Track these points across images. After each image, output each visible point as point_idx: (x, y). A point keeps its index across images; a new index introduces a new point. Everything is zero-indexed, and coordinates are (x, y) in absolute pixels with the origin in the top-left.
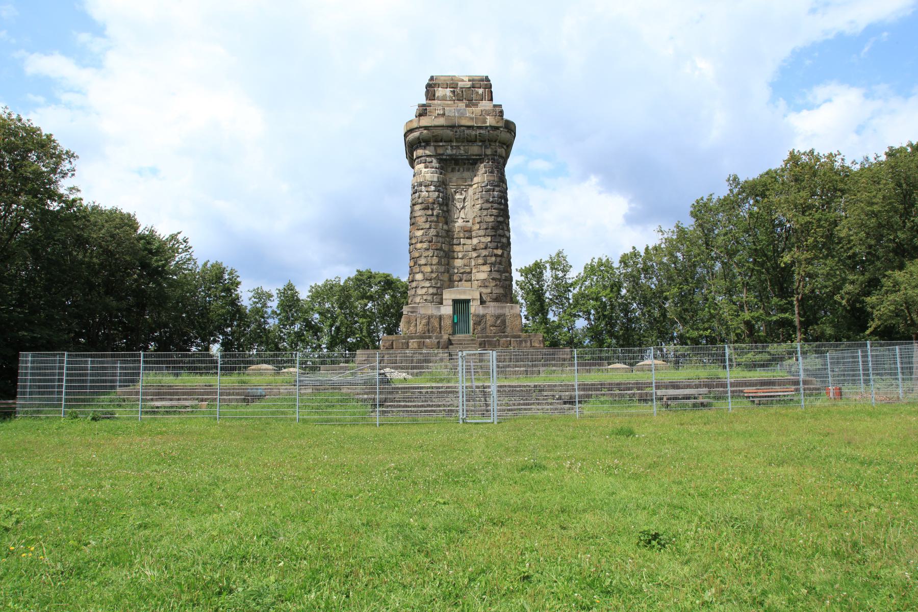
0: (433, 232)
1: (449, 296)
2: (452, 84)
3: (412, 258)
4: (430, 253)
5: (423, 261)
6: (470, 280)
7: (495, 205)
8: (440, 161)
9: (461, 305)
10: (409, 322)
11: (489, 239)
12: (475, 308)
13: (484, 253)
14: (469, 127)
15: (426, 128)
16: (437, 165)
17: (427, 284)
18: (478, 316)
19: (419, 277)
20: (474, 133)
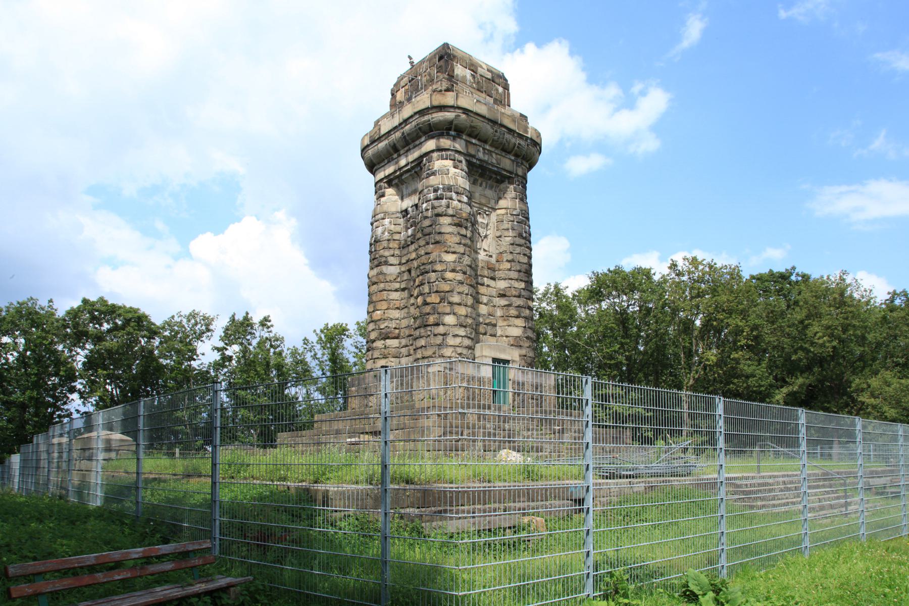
0: (467, 260)
1: (486, 351)
6: (495, 336)
8: (470, 164)
12: (513, 374)
14: (511, 131)
16: (465, 168)
17: (462, 332)
20: (513, 140)
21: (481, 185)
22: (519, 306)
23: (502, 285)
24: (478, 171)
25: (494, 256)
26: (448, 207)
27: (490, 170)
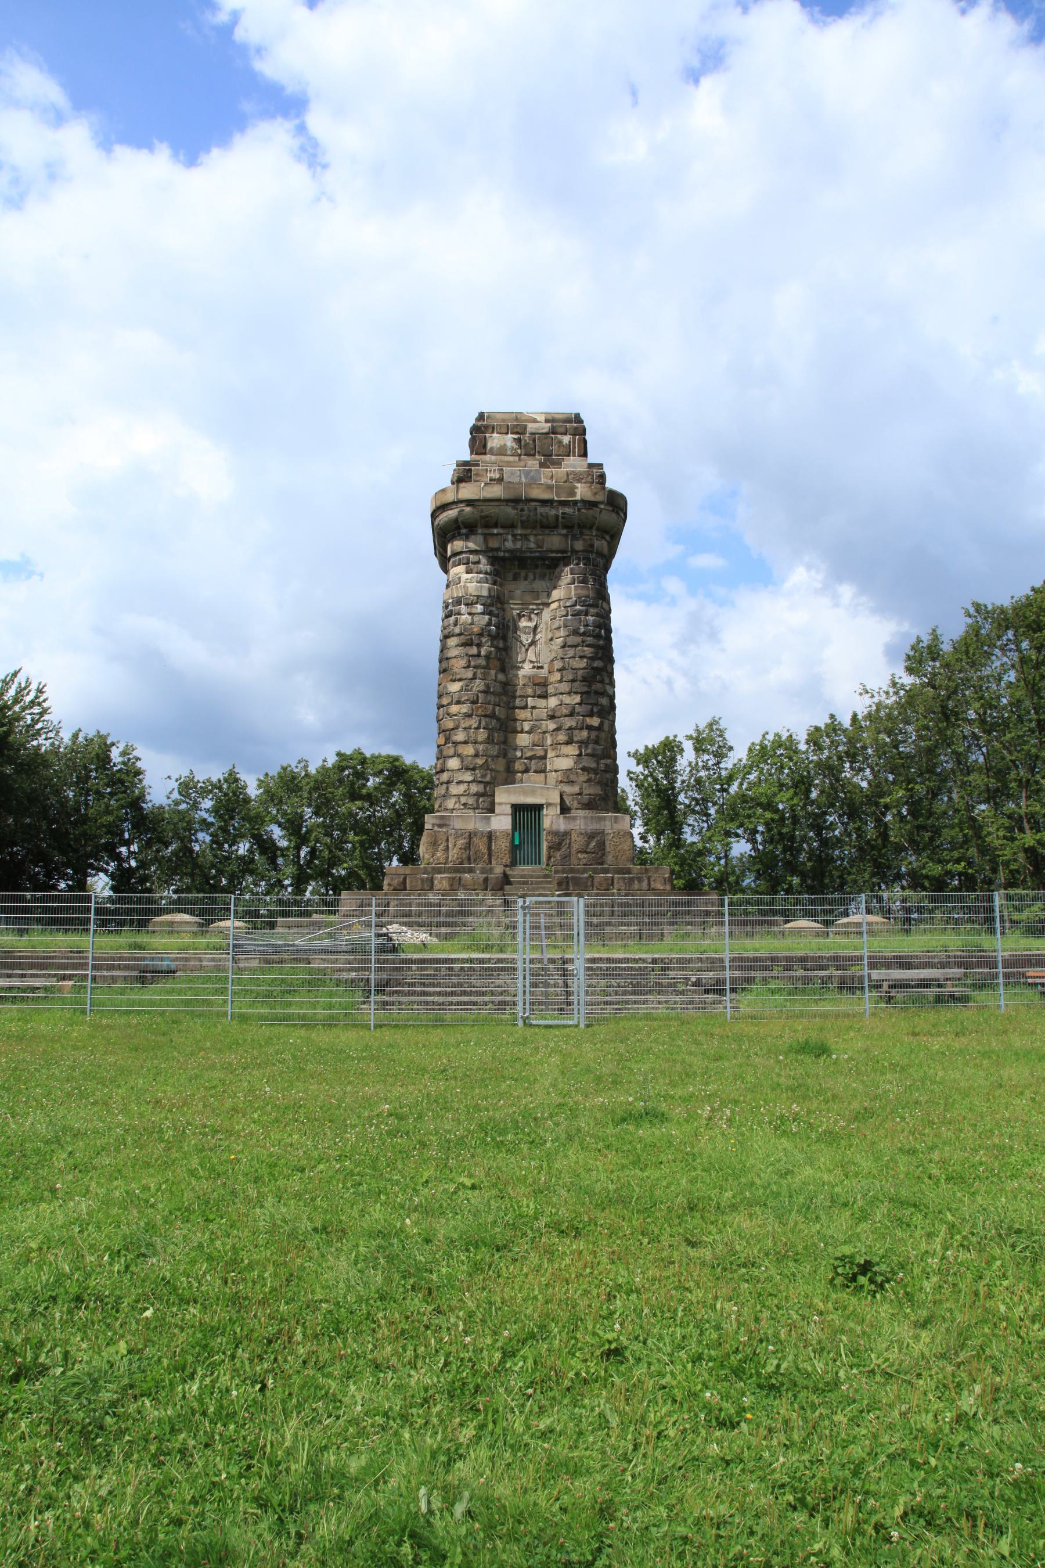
0: (478, 685)
1: (505, 797)
2: (516, 425)
3: (442, 731)
4: (473, 722)
5: (460, 736)
6: (544, 771)
7: (589, 640)
8: (493, 560)
10: (434, 844)
11: (577, 699)
12: (551, 820)
13: (569, 723)
15: (469, 502)
16: (488, 568)
17: (468, 777)
18: (556, 833)
19: (453, 763)
20: (553, 512)
21: (526, 578)
22: (570, 728)
23: (553, 702)
25: (546, 666)
26: (456, 624)
27: (532, 558)
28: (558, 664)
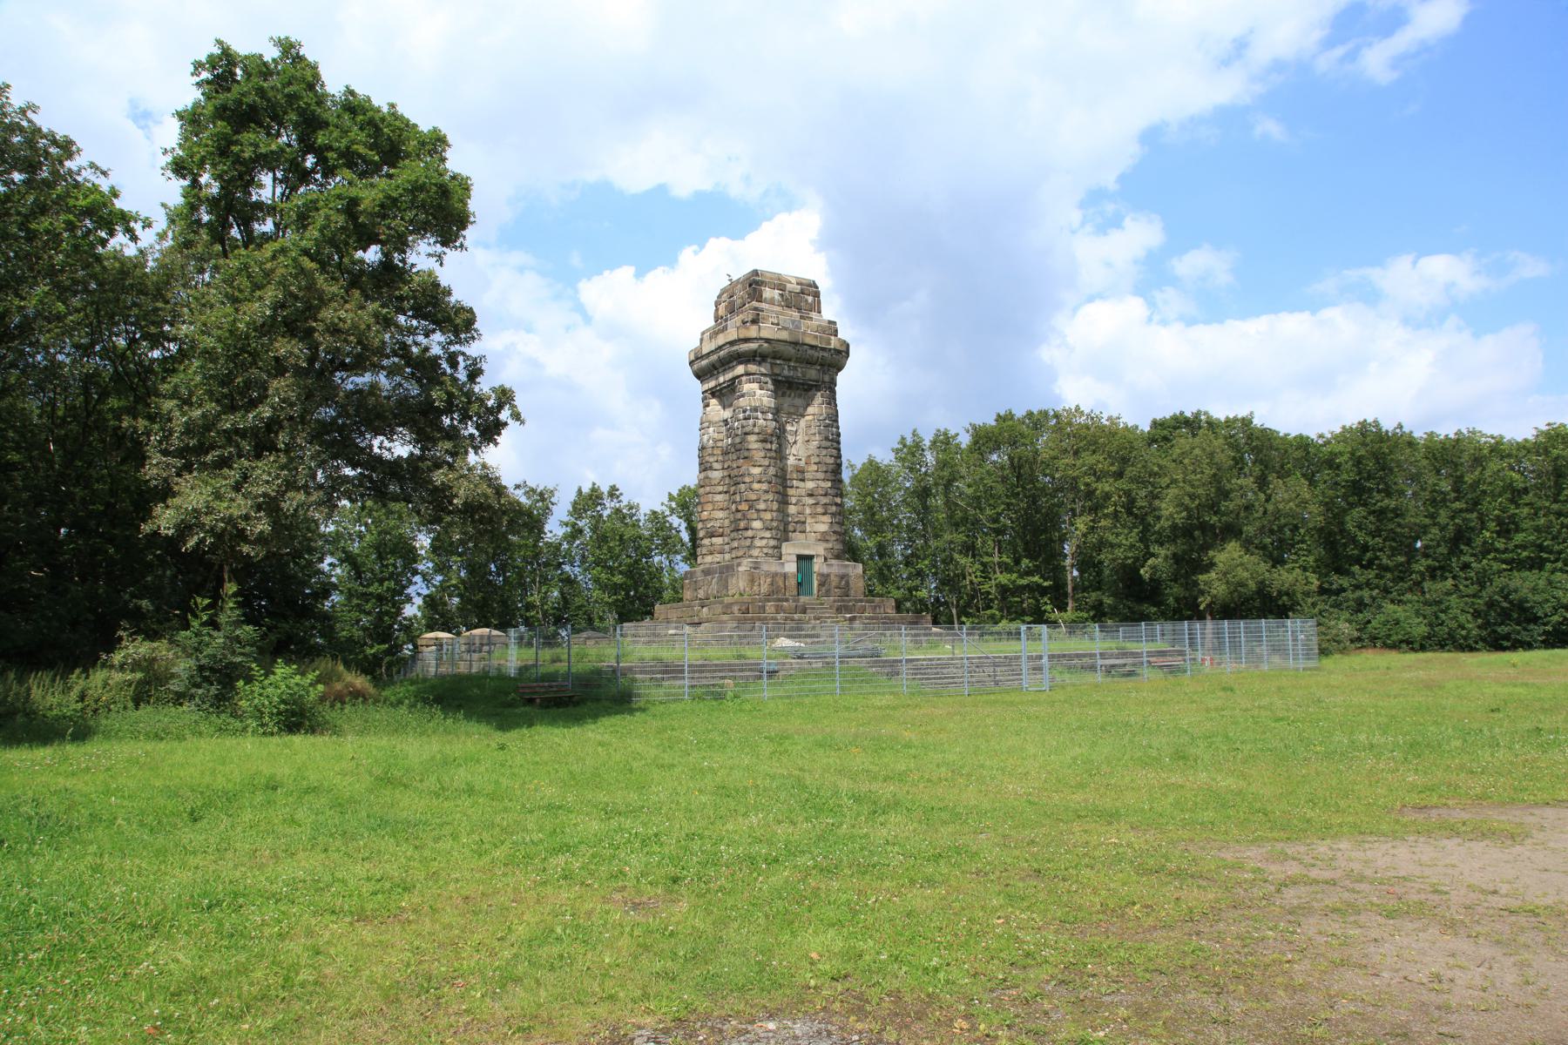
0: (772, 471)
1: (790, 551)
2: (780, 284)
4: (770, 496)
8: (776, 382)
9: (805, 560)
11: (829, 484)
12: (818, 566)
13: (824, 500)
14: (812, 347)
15: (767, 340)
17: (768, 534)
23: (810, 485)
24: (782, 386)
28: (814, 459)
